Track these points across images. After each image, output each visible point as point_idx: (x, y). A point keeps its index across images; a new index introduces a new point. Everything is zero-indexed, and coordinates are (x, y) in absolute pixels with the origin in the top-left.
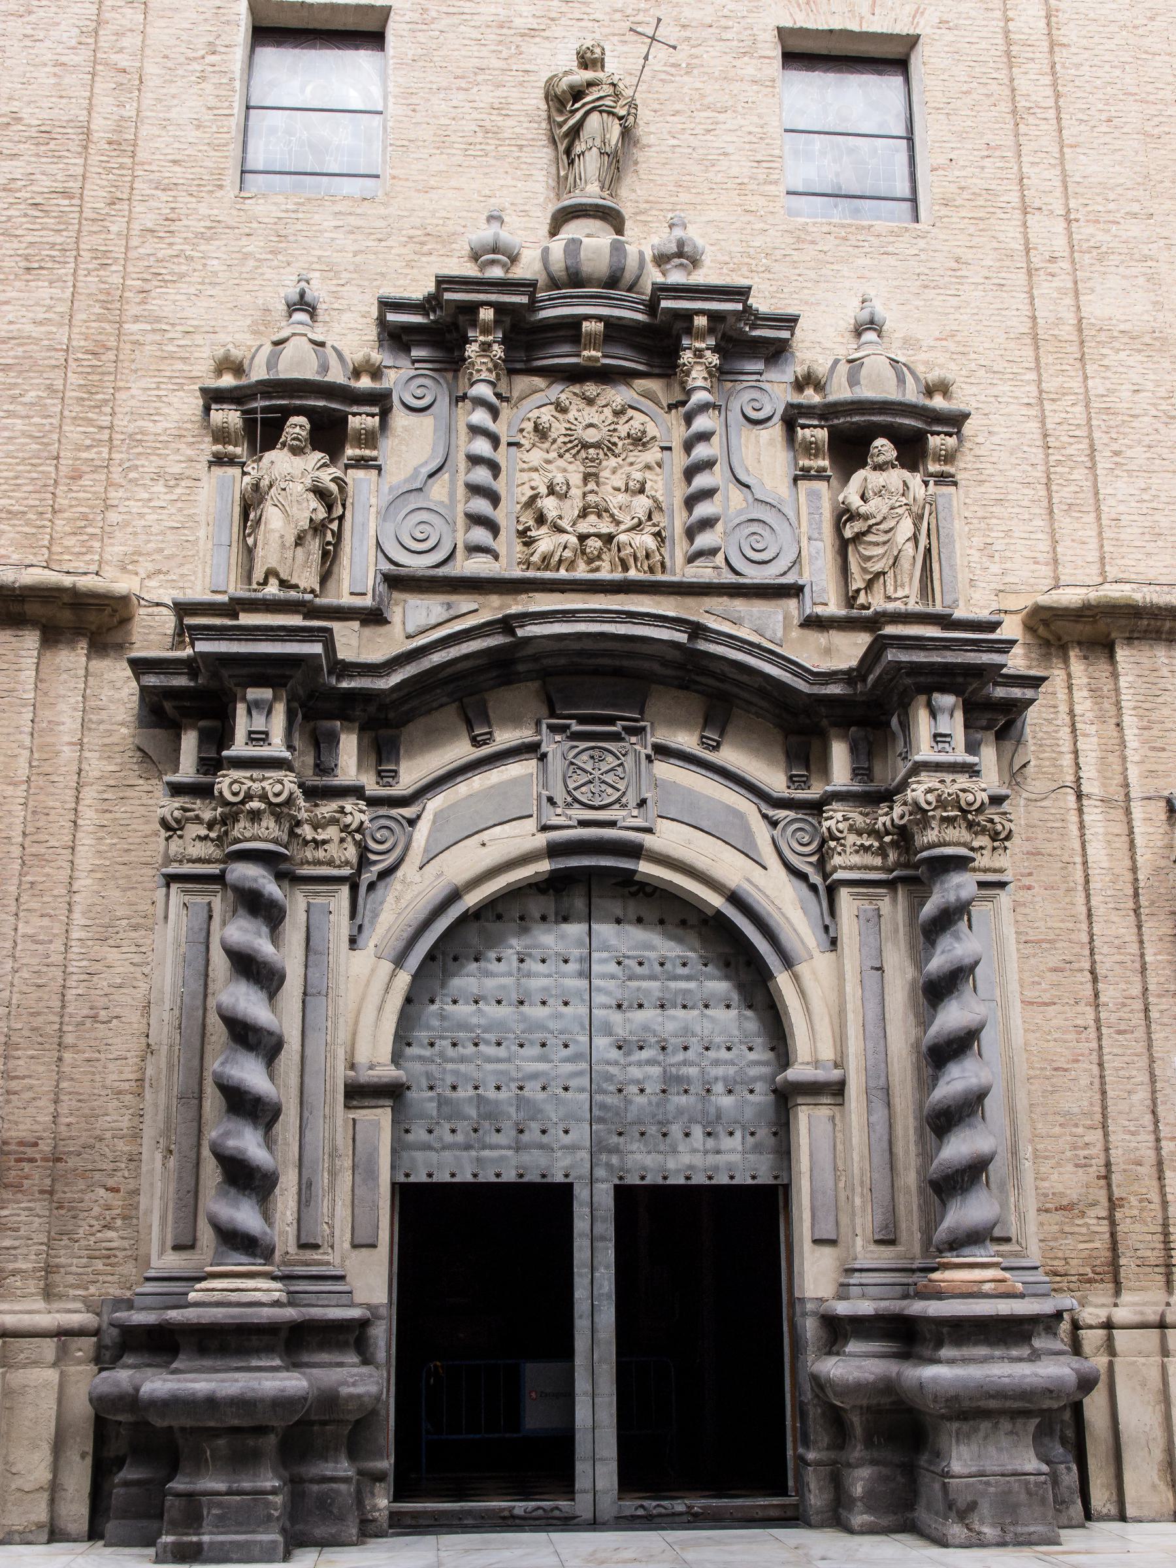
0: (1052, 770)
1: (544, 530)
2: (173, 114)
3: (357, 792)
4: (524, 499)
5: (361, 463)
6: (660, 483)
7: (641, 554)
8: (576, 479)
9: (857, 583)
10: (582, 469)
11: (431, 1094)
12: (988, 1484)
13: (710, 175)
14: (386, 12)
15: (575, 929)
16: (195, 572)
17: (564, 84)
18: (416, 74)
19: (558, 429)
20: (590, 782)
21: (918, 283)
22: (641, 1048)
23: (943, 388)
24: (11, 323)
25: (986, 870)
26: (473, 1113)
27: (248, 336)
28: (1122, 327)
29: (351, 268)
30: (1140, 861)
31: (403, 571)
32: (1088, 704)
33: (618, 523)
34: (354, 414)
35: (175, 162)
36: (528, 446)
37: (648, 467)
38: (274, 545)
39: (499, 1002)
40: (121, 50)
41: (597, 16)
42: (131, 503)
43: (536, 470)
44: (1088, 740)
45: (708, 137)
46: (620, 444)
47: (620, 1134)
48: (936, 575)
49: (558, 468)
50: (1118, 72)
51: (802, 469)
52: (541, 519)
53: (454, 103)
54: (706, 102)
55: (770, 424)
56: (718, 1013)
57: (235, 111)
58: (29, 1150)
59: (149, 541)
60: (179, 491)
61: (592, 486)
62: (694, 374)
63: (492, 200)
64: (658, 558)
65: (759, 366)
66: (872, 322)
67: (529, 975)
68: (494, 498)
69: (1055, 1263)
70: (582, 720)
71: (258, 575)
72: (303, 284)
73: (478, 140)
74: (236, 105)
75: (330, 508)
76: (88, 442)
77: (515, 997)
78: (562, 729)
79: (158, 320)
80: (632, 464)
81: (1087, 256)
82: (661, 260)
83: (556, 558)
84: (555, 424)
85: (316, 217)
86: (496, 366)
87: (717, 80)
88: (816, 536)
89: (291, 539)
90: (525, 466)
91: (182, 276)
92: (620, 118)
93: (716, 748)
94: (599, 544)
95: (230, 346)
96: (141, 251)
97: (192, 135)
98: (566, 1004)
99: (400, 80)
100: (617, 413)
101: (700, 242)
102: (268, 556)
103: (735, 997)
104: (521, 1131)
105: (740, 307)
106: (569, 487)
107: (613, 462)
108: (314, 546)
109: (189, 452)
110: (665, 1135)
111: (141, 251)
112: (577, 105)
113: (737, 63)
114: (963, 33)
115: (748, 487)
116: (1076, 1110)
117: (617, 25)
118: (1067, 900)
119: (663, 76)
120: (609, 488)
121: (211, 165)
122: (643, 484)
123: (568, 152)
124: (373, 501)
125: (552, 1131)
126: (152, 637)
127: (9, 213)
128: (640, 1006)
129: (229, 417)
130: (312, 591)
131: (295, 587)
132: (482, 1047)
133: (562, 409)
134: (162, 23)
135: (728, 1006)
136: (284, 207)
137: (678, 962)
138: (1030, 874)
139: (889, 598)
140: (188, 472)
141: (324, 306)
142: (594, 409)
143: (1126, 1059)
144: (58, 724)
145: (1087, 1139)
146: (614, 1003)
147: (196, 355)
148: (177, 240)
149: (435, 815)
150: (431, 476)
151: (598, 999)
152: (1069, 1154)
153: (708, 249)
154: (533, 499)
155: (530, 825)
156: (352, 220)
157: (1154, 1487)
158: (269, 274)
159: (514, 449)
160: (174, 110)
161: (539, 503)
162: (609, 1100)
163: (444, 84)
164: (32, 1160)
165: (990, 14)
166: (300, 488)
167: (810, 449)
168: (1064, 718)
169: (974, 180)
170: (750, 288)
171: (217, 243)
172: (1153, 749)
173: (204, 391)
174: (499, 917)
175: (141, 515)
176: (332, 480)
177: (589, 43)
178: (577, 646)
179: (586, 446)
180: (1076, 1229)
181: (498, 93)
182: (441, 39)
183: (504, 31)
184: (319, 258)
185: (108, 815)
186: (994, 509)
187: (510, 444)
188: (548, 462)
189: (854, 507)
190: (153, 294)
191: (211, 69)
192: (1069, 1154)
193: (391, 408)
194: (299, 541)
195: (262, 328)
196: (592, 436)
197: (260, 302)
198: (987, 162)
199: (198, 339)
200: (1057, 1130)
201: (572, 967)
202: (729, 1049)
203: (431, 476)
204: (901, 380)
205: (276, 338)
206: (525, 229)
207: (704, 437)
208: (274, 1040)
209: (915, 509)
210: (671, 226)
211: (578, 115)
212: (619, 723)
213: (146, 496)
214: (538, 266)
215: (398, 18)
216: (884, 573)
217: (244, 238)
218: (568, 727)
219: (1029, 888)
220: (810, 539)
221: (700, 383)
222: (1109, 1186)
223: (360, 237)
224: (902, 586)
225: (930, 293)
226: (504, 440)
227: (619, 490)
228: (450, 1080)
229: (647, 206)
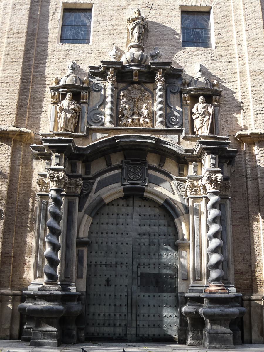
0: (240, 172)
3: (79, 176)
5: (84, 103)
11: (96, 245)
12: (218, 335)
15: (130, 209)
17: (130, 19)
20: (133, 174)
22: (144, 235)
24: (8, 73)
25: (224, 195)
26: (106, 249)
28: (258, 71)
30: (260, 193)
32: (249, 157)
34: (82, 92)
39: (112, 224)
40: (35, 14)
41: (140, 3)
42: (33, 112)
44: (249, 165)
45: (164, 29)
47: (139, 254)
48: (214, 128)
50: (257, 14)
53: (107, 23)
56: (162, 227)
58: (7, 254)
65: (175, 80)
67: (119, 218)
69: (238, 285)
70: (132, 161)
75: (76, 113)
76: (24, 99)
77: (116, 223)
78: (128, 163)
79: (41, 72)
81: (250, 55)
82: (152, 57)
83: (127, 124)
92: (143, 26)
93: (163, 167)
98: (128, 225)
103: (166, 224)
104: (117, 253)
110: (149, 255)
112: (134, 23)
113: (171, 13)
117: (144, 5)
119: (154, 16)
123: (132, 34)
125: (124, 253)
126: (37, 142)
127: (9, 50)
128: (144, 225)
132: (108, 234)
135: (165, 226)
137: (153, 215)
138: (235, 196)
144: (16, 161)
146: (138, 225)
149: (98, 182)
151: (135, 224)
152: (242, 260)
154: (122, 111)
155: (119, 184)
156: (83, 50)
157: (259, 336)
161: (123, 112)
162: (137, 247)
164: (8, 257)
168: (243, 160)
170: (171, 63)
174: (113, 205)
175: (36, 115)
178: (131, 144)
180: (243, 278)
182: (105, 10)
183: (118, 7)
185: (26, 181)
186: (228, 112)
189: (195, 113)
201: (129, 217)
202: (165, 235)
208: (59, 232)
212: (141, 161)
213: (37, 111)
218: (129, 162)
219: (235, 199)
220: (185, 119)
222: (251, 268)
225: (213, 64)
228: (101, 242)
229: (149, 45)
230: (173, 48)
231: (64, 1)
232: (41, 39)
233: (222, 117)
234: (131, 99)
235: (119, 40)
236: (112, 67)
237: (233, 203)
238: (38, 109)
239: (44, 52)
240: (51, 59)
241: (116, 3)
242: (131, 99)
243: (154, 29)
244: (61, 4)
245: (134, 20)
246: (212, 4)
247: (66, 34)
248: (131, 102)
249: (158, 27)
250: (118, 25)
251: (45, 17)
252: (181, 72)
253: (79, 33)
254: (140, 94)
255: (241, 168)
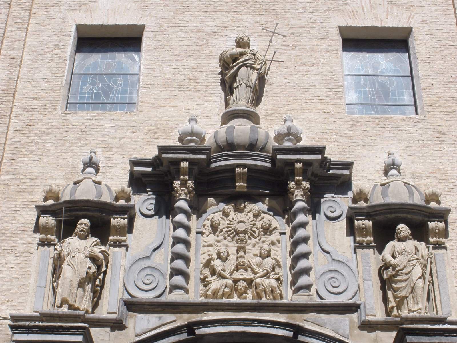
1: (215, 277)
2: (35, 77)
4: (204, 261)
6: (280, 252)
7: (268, 290)
8: (233, 250)
9: (392, 303)
10: (236, 245)
13: (306, 96)
14: (142, 28)
16: (26, 301)
18: (156, 54)
19: (223, 224)
21: (418, 145)
23: (435, 197)
27: (63, 180)
29: (118, 146)
31: (134, 299)
33: (255, 273)
35: (34, 98)
36: (207, 233)
37: (273, 243)
38: (67, 285)
41: (247, 25)
43: (210, 246)
45: (304, 78)
46: (257, 231)
49: (224, 245)
51: (358, 242)
52: (213, 272)
53: (174, 67)
54: (302, 62)
55: (340, 219)
57: (66, 74)
59: (4, 285)
60: (21, 259)
61: (241, 253)
62: (296, 193)
63: (192, 112)
64: (278, 291)
66: (393, 164)
68: (187, 260)
71: (58, 302)
72: (93, 154)
73: (185, 84)
74: (66, 72)
75: (99, 267)
79: (19, 173)
80: (263, 242)
82: (279, 137)
83: (221, 292)
84: (222, 222)
85: (102, 122)
86: (189, 192)
87: (308, 51)
88: (368, 278)
89: (76, 283)
90: (206, 244)
91: (32, 152)
92: (257, 70)
94: (245, 284)
95: (53, 185)
96: (13, 140)
97: (44, 86)
99: (147, 57)
100: (256, 216)
101: (300, 128)
102: (62, 292)
105: (319, 157)
106: (228, 255)
107: (253, 240)
108: (89, 287)
109: (28, 239)
111: (13, 140)
112: (235, 64)
113: (319, 43)
114: (434, 25)
115: (328, 253)
117: (257, 29)
120: (251, 255)
121: (51, 99)
122: (269, 252)
124: (123, 263)
129: (49, 220)
130: (87, 312)
131: (77, 309)
133: (226, 214)
134: (34, 36)
136: (85, 118)
139: (410, 311)
140: (26, 249)
141: (103, 165)
142: (243, 214)
147: (36, 190)
148: (32, 135)
150: (155, 250)
153: (304, 131)
156: (120, 123)
158: (76, 149)
159: (200, 235)
160: (36, 75)
161: (212, 263)
163: (169, 58)
165: (447, 17)
166: (82, 255)
167: (363, 231)
169: (446, 94)
171: (51, 136)
173: (37, 207)
176: (100, 252)
177: (241, 35)
179: (238, 233)
181: (195, 62)
183: (200, 33)
184: (102, 141)
187: (198, 233)
188: (218, 241)
190: (17, 161)
191: (55, 56)
193: (135, 215)
194: (81, 285)
195: (70, 176)
196: (241, 227)
197: (70, 163)
198: (451, 85)
199: (38, 182)
203: (155, 250)
204: (411, 193)
205: (75, 180)
206: (209, 125)
207: (303, 225)
209: (422, 261)
210: (285, 121)
211: (235, 68)
213: (4, 261)
214: (213, 140)
215: (148, 30)
216: (407, 297)
217: (65, 133)
221: (299, 197)
223: (123, 131)
224: (417, 304)
225: (425, 150)
226: (194, 231)
227: (256, 255)
229: (272, 112)
230: (326, 118)
231: (78, 23)
232: (23, 102)
233: (454, 272)
234: (229, 233)
235: (201, 102)
236: (186, 160)
238: (8, 258)
239: (29, 130)
240: (44, 144)
241: (195, 24)
242: (231, 234)
243: (283, 79)
244: (73, 29)
245: (235, 57)
246: (413, 23)
247: (82, 90)
248: (230, 242)
249: (290, 73)
250: (199, 70)
251: (36, 55)
252: (347, 169)
253: (110, 88)
254: (252, 221)
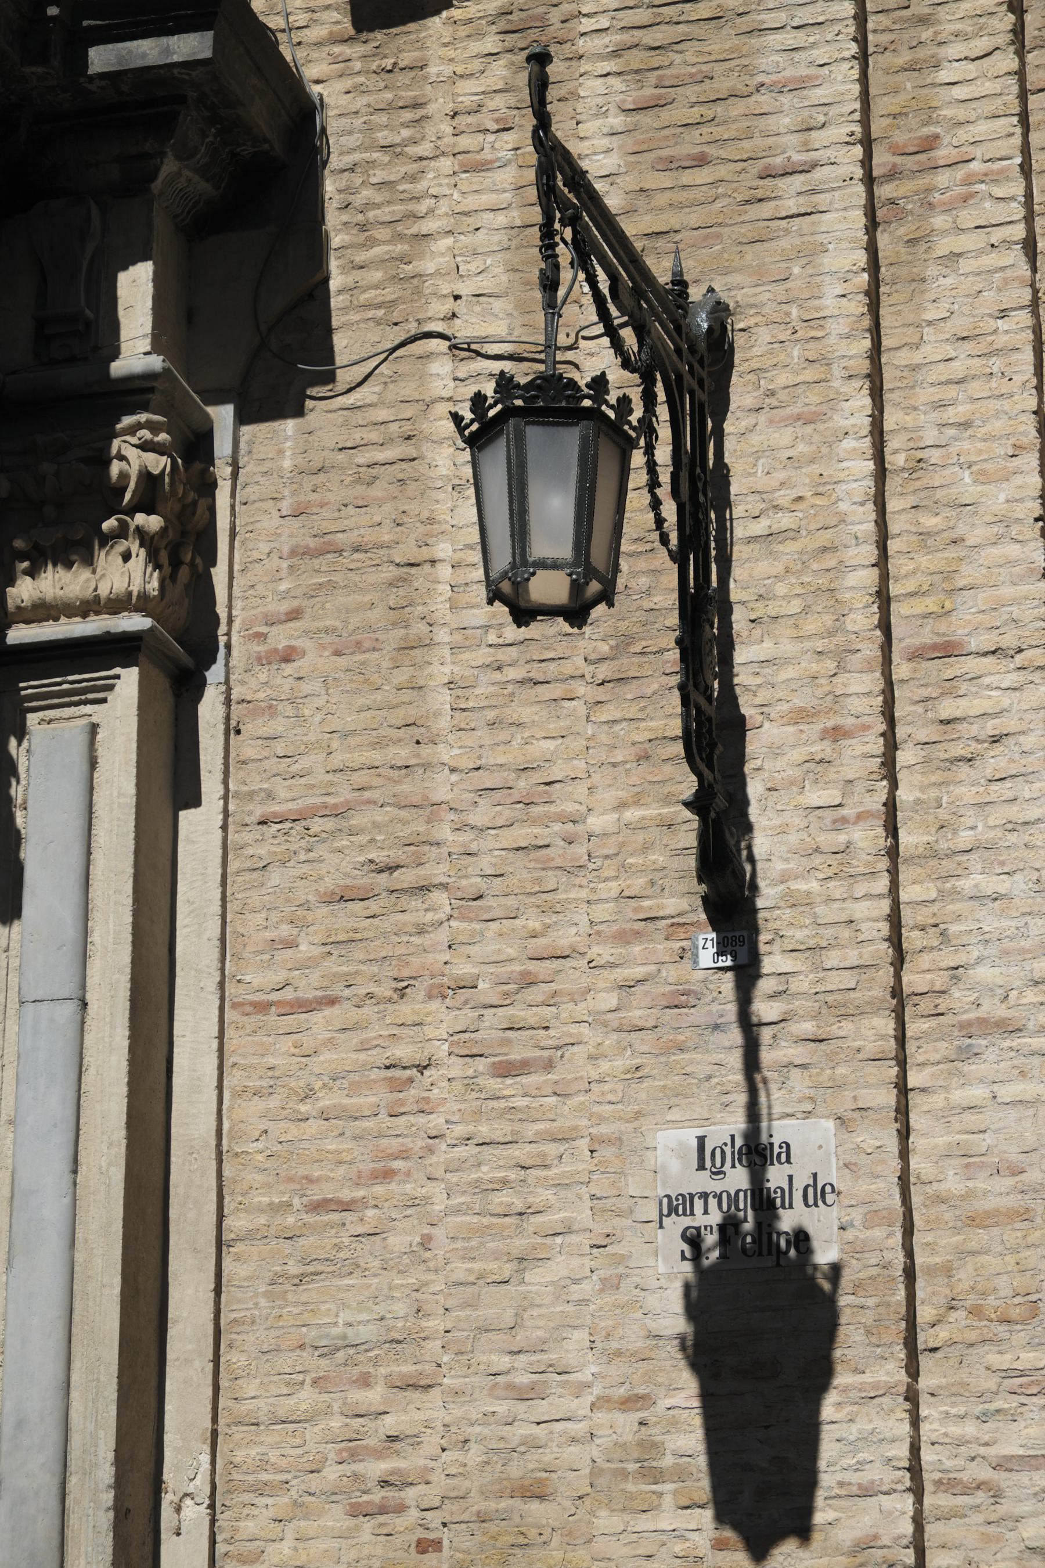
116: (367, 1332)
118: (401, 676)
138: (294, 615)
143: (520, 1153)
145: (390, 1424)
172: (670, 165)
192: (332, 1473)
200: (306, 1399)
219: (288, 656)
237: (271, 710)
255: (400, 237)
